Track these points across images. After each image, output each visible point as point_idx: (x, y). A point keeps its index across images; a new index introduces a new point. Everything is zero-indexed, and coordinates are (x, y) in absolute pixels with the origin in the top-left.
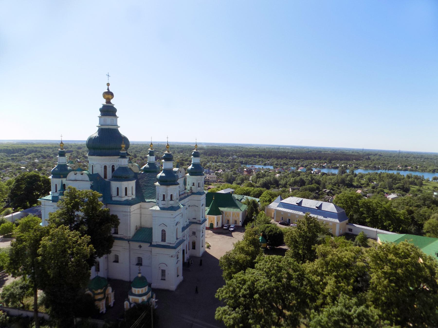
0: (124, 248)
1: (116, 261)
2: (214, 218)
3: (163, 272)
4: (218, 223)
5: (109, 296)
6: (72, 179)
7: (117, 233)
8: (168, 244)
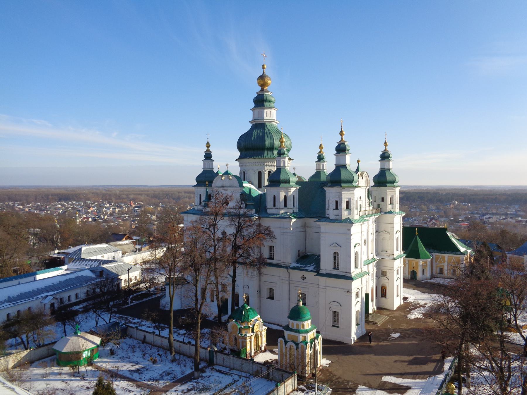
0: (283, 280)
1: (272, 297)
2: (417, 263)
3: (335, 314)
4: (423, 271)
5: (259, 333)
6: (219, 186)
7: (273, 259)
8: (343, 274)
